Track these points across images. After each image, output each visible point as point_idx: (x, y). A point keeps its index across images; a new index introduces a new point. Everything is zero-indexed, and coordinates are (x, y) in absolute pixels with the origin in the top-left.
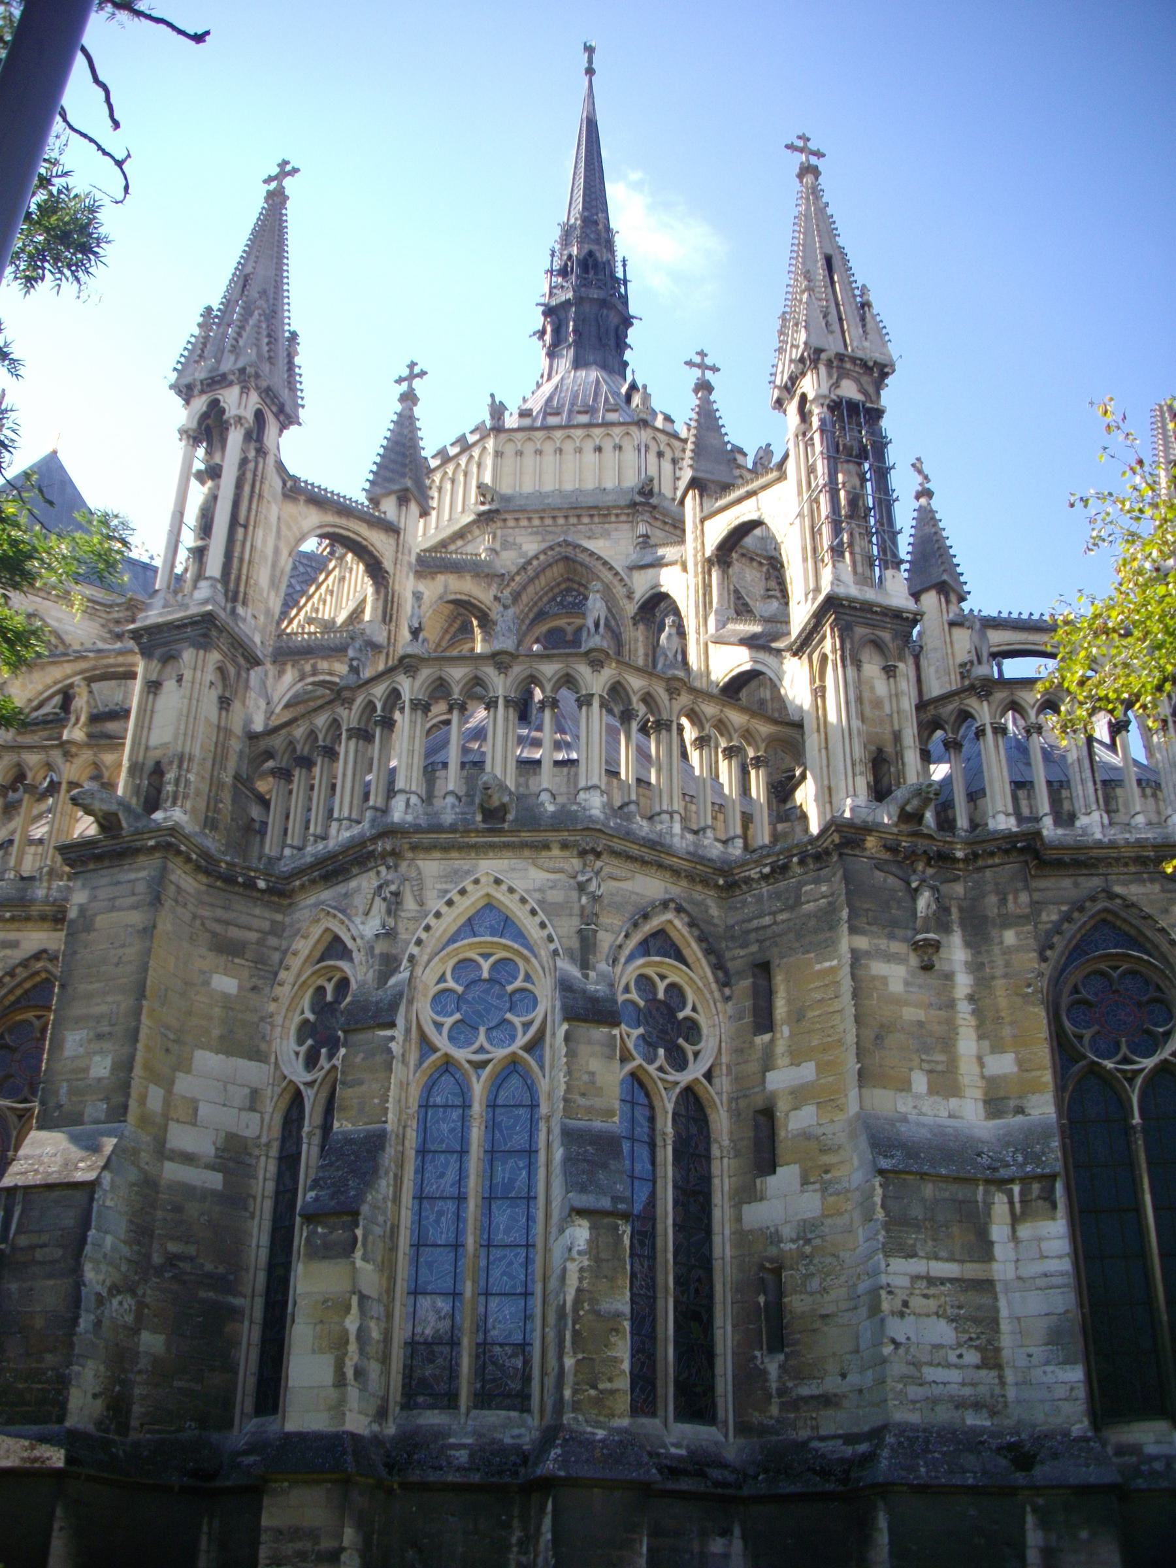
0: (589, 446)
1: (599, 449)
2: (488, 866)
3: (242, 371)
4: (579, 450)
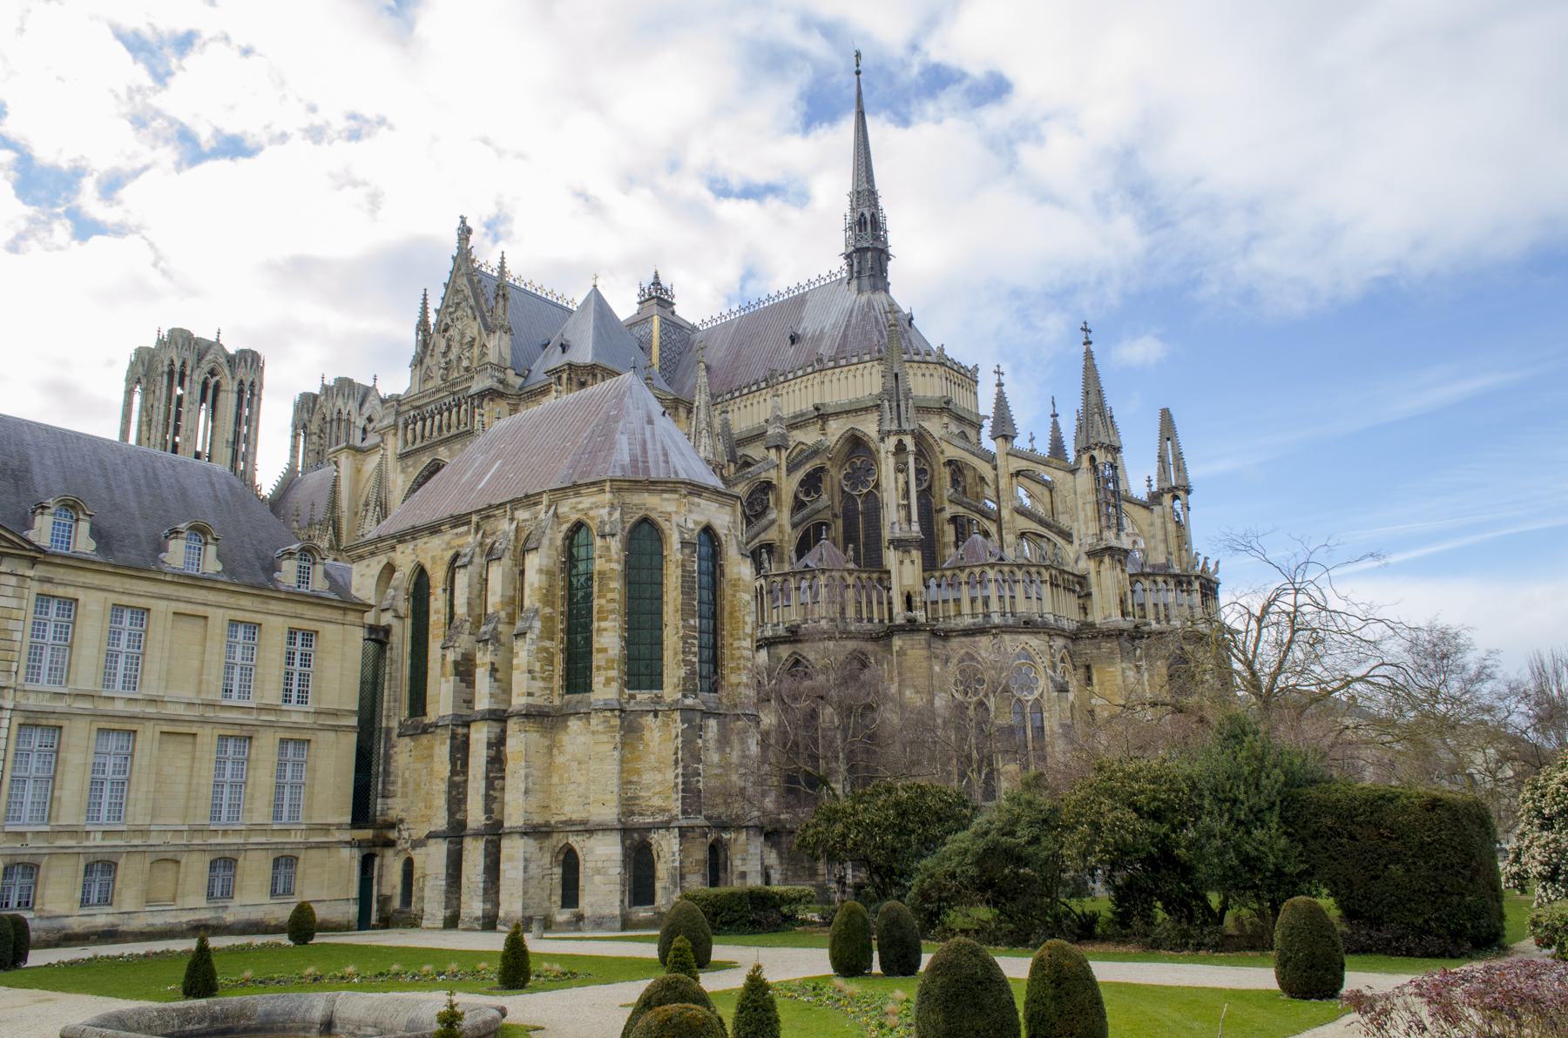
0: (919, 373)
1: (924, 375)
2: (1023, 638)
3: (913, 430)
4: (915, 374)
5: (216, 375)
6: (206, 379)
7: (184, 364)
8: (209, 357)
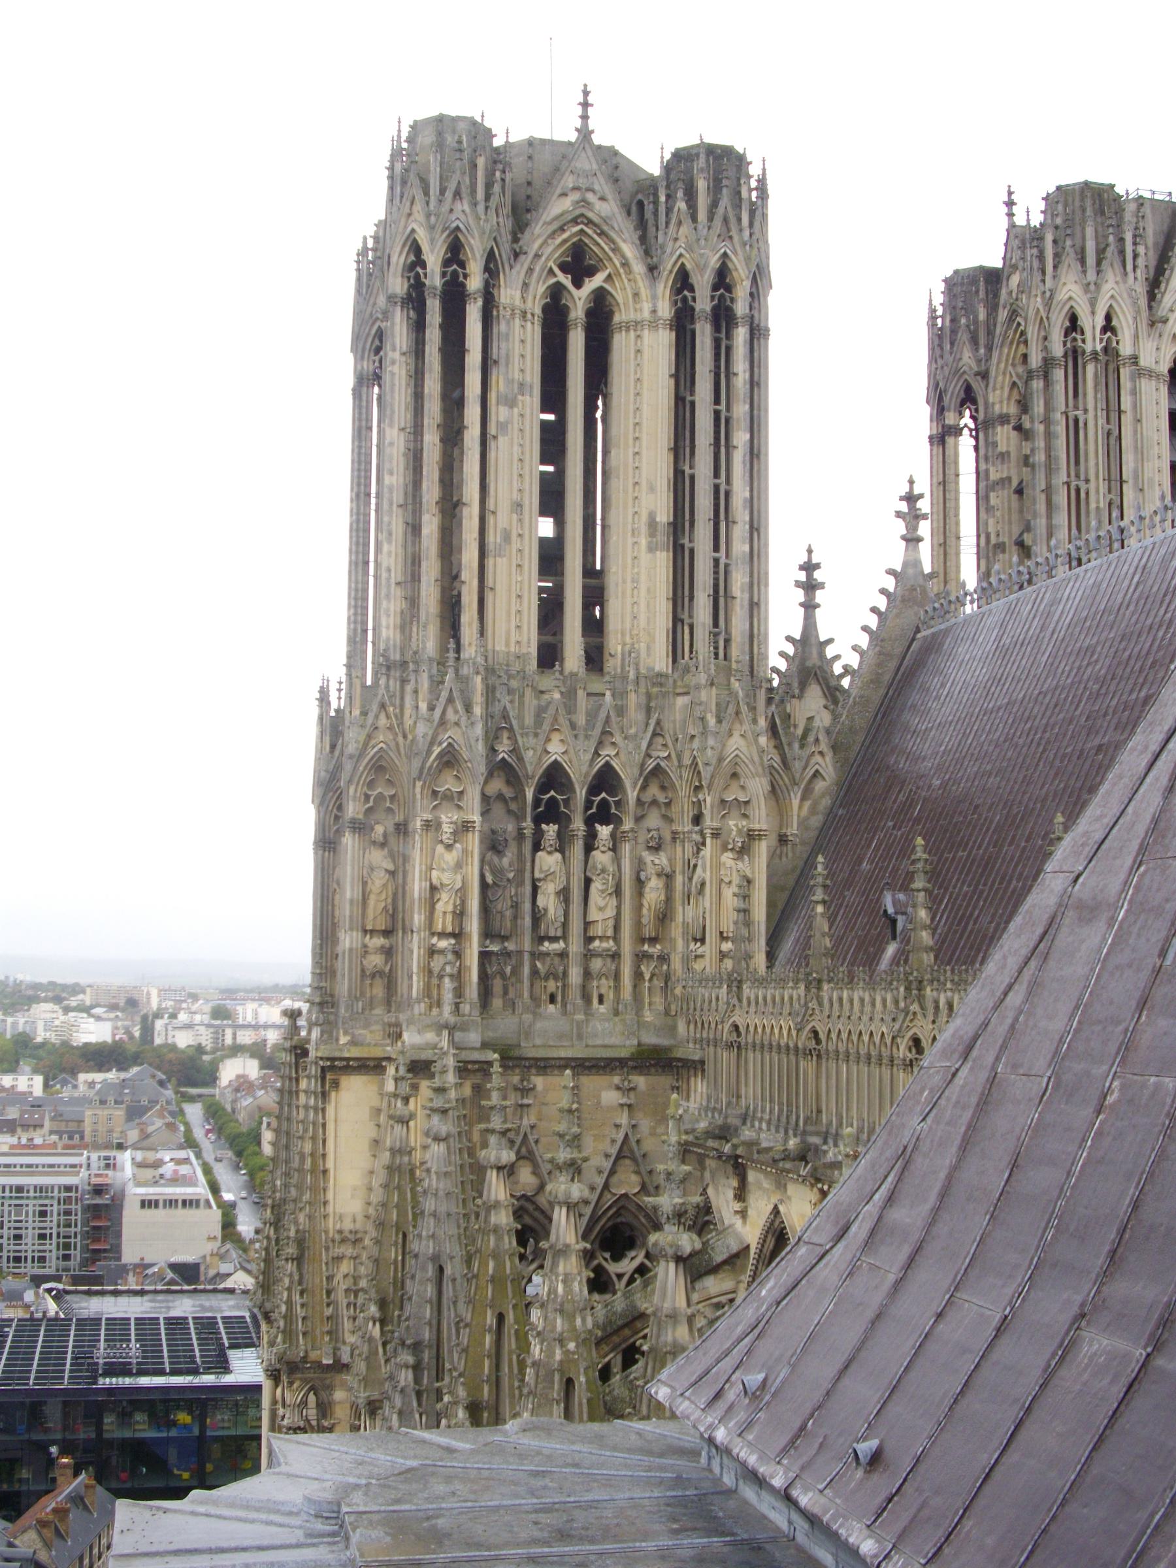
5: (591, 272)
6: (556, 291)
7: (455, 253)
8: (559, 206)
